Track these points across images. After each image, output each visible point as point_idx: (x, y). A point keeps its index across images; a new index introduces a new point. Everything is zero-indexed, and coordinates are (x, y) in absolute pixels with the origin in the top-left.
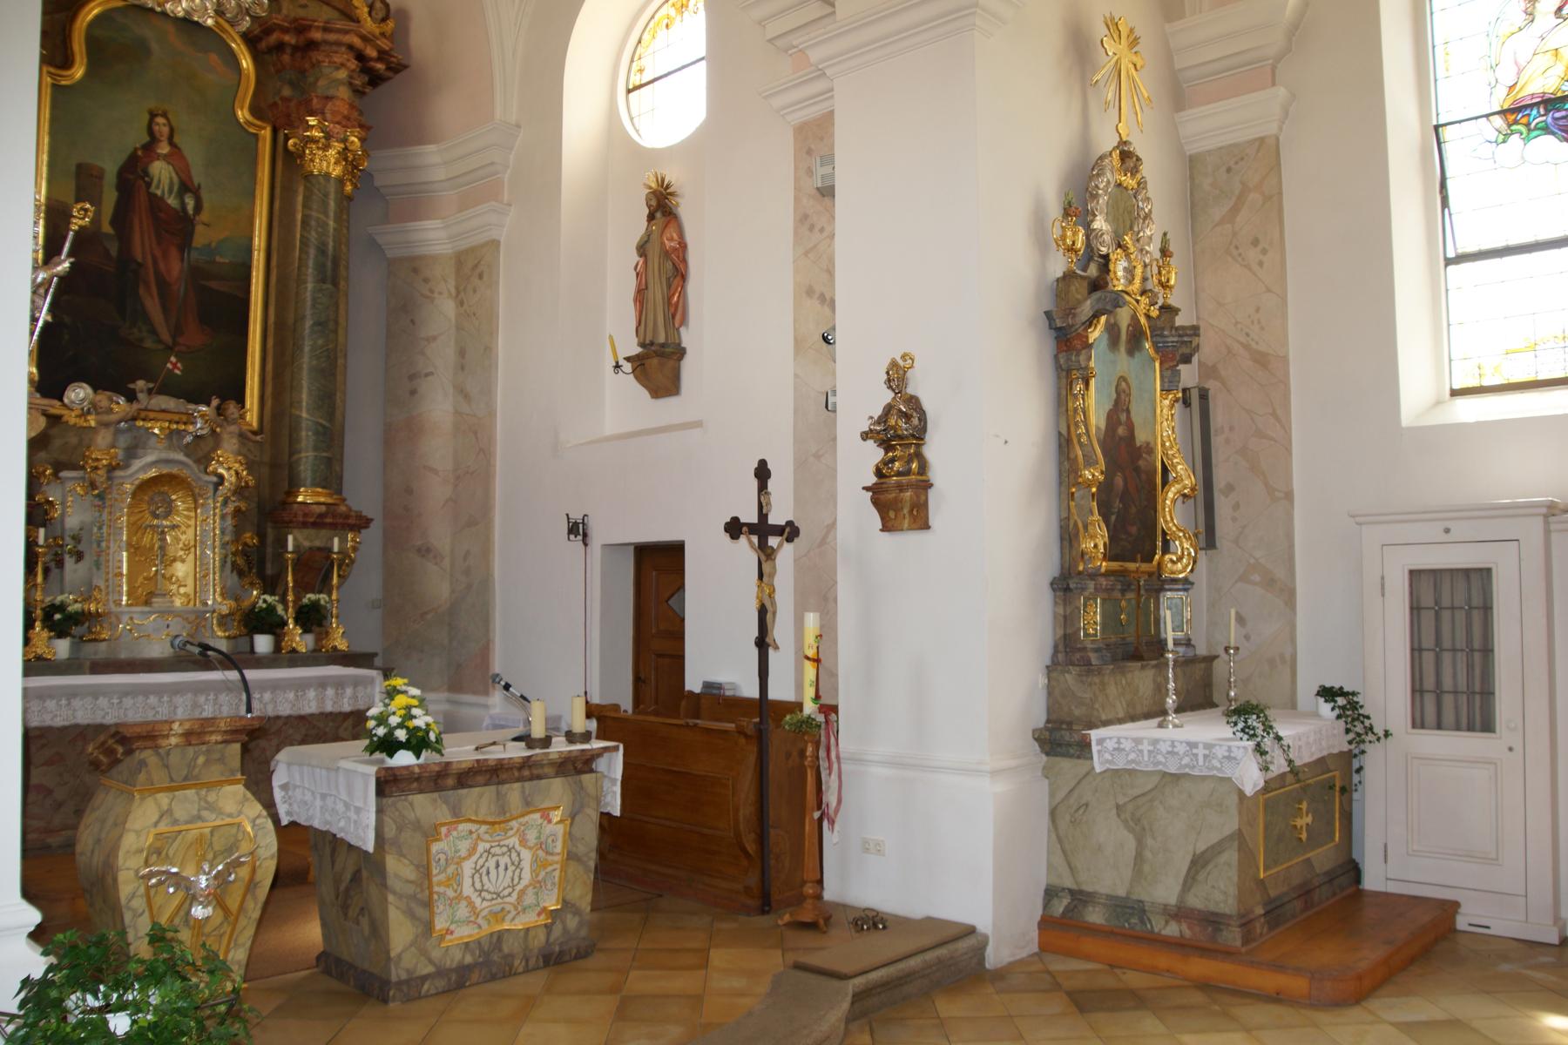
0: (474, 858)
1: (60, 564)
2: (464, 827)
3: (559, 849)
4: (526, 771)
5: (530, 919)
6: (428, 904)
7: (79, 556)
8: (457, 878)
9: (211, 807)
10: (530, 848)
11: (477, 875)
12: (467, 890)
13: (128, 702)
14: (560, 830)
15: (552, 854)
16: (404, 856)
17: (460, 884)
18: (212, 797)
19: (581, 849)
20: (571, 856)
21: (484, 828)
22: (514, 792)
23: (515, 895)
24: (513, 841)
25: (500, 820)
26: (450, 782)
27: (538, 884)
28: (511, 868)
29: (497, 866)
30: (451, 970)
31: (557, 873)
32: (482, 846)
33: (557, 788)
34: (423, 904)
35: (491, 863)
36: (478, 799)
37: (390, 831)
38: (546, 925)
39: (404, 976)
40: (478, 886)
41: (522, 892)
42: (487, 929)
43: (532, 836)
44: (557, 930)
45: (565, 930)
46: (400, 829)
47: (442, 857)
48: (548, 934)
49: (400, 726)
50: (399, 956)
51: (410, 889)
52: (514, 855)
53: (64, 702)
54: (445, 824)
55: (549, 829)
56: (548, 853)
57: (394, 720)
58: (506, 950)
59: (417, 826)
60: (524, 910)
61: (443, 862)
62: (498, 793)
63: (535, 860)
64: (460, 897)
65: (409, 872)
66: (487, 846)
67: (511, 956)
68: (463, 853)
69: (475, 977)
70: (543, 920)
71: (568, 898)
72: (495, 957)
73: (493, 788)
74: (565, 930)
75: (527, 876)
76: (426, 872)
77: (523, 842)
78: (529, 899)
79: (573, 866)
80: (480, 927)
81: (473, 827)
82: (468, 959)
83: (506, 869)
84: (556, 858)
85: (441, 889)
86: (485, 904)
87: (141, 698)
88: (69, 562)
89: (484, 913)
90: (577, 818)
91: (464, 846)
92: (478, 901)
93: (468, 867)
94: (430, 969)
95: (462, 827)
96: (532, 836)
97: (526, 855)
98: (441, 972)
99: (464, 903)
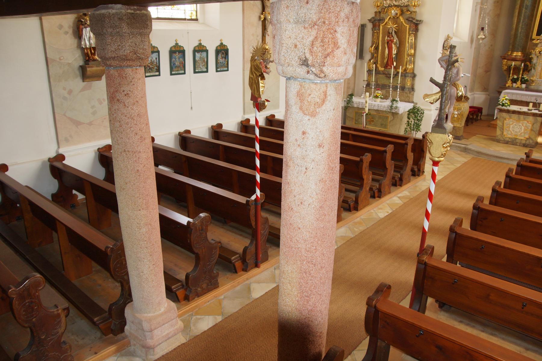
0: (513, 125)
1: (531, 70)
2: (511, 120)
3: (530, 128)
4: (524, 113)
5: (522, 138)
6: (503, 129)
7: (534, 69)
8: (509, 128)
9: (459, 105)
10: (524, 126)
11: (513, 128)
12: (511, 129)
13: (523, 97)
14: (530, 125)
15: (528, 129)
16: (500, 121)
17: (510, 128)
18: (460, 104)
19: (535, 130)
20: (532, 130)
21: (515, 121)
22: (522, 117)
23: (519, 134)
24: (521, 124)
25: (519, 120)
26: (511, 112)
27: (525, 133)
28: (520, 129)
29: (517, 127)
30: (506, 141)
31: (529, 132)
32: (514, 124)
33: (531, 118)
34: (502, 129)
35: (516, 127)
36: (515, 116)
37: (499, 117)
38: (525, 140)
39: (498, 139)
40: (513, 129)
41: (521, 133)
42: (513, 137)
43: (524, 125)
44: (528, 142)
45: (529, 142)
46: (500, 117)
47: (507, 123)
48: (526, 142)
49: (501, 102)
50: (498, 136)
51: (501, 127)
52: (520, 127)
53: (511, 95)
54: (508, 118)
55: (528, 124)
56: (527, 128)
57: (501, 101)
58: (517, 141)
59: (503, 117)
60: (521, 136)
61: (507, 123)
62: (519, 116)
63: (525, 129)
64: (509, 130)
65: (501, 124)
66: (516, 124)
67: (518, 142)
68: (511, 124)
69: (510, 143)
70: (525, 139)
71: (531, 137)
72: (515, 142)
73: (518, 115)
74: (529, 142)
75: (523, 131)
76: (503, 124)
77: (523, 125)
78: (523, 135)
79: (533, 132)
80: (512, 136)
81: (513, 120)
82: (510, 140)
83: (519, 128)
84: (529, 130)
85: (506, 128)
86: (514, 133)
87: (525, 97)
88: (533, 69)
89: (514, 134)
90: (535, 124)
91: (511, 123)
92: (513, 132)
93: (511, 126)
94: (503, 139)
95: (511, 120)
96: (524, 125)
97: (523, 128)
98: (504, 140)
99: (510, 131)
